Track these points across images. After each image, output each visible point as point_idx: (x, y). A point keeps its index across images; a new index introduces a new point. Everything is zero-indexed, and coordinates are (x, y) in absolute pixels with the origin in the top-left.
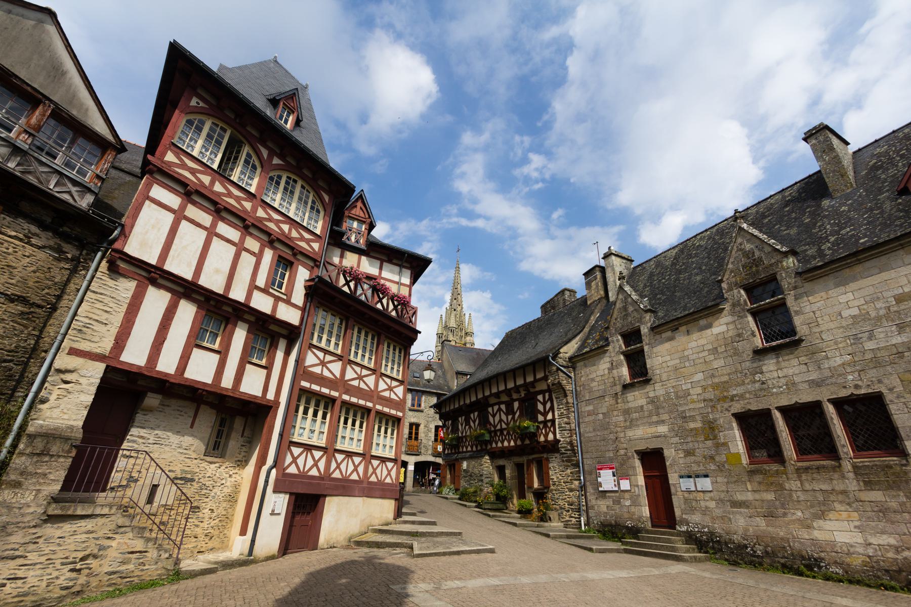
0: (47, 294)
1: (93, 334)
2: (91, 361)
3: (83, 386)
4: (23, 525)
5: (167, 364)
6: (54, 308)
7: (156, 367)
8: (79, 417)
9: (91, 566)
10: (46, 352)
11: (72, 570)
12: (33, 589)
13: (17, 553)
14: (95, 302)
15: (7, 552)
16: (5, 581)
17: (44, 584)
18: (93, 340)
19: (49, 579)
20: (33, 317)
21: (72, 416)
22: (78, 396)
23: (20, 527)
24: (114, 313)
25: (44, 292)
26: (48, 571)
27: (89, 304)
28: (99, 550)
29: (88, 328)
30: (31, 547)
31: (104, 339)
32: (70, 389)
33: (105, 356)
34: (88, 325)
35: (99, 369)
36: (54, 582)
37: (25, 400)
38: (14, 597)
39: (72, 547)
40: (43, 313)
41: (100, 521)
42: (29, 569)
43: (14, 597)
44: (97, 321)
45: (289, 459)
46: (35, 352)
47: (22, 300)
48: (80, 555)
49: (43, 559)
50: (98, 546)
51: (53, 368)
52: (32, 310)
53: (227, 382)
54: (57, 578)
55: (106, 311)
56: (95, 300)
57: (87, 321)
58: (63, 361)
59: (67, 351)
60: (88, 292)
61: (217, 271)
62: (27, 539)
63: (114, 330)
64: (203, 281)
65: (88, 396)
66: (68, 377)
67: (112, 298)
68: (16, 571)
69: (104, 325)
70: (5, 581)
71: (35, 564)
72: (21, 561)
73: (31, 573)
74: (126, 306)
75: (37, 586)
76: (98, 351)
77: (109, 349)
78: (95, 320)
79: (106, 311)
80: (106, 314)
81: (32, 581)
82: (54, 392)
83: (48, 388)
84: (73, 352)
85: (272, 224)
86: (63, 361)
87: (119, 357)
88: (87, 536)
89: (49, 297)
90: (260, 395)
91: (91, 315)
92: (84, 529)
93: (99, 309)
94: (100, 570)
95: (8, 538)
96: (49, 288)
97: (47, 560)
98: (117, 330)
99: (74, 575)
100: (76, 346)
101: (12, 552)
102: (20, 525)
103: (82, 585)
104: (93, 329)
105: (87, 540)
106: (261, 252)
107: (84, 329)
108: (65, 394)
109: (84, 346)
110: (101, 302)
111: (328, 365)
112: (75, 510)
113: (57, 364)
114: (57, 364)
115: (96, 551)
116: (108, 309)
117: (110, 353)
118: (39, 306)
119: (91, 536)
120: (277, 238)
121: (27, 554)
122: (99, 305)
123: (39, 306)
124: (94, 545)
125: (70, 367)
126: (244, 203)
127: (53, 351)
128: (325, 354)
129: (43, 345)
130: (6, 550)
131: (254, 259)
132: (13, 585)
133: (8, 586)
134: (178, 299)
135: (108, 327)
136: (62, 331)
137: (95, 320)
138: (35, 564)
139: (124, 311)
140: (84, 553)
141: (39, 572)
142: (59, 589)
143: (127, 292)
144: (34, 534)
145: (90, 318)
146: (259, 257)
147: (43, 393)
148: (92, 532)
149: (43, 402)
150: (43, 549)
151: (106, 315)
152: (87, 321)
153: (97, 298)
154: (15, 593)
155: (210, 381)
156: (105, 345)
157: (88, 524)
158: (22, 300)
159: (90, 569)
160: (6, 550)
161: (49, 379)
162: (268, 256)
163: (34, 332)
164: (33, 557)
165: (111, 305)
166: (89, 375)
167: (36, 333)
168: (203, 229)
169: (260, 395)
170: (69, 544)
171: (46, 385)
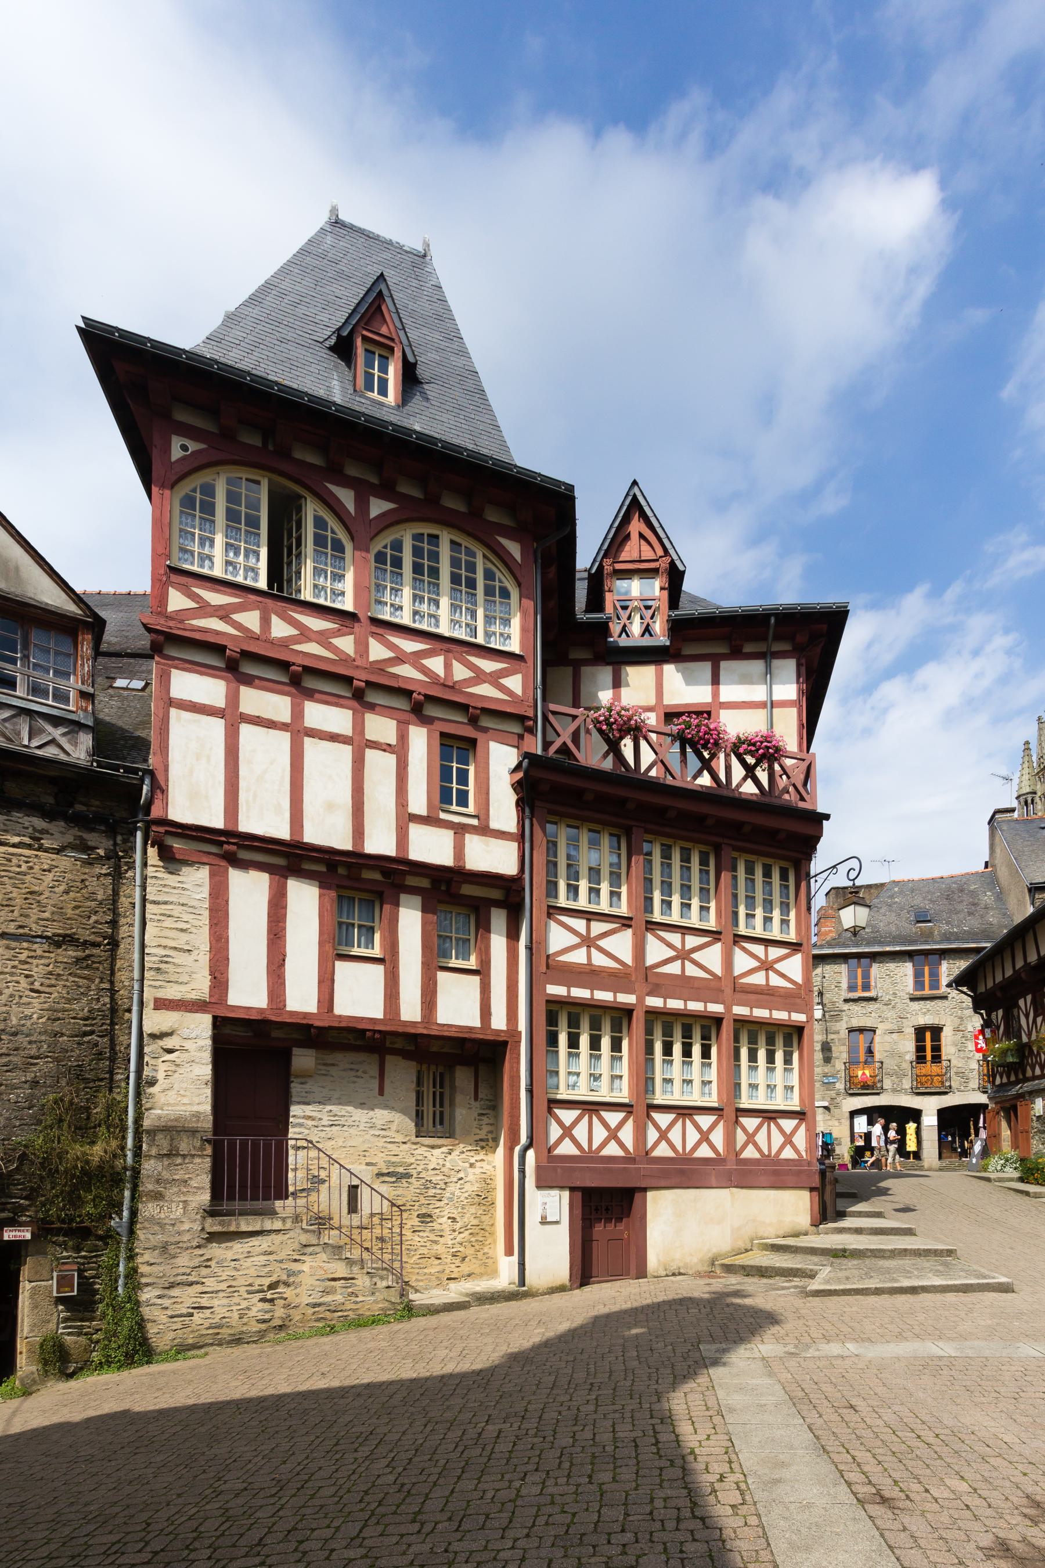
2: (188, 1014)
8: (202, 1098)
10: (129, 1011)
12: (224, 1320)
13: (191, 1279)
15: (180, 1277)
24: (193, 930)
27: (155, 924)
29: (166, 962)
31: (194, 976)
33: (205, 1001)
35: (201, 1026)
37: (128, 1084)
38: (207, 1329)
43: (207, 1329)
44: (175, 948)
45: (555, 1132)
46: (115, 1013)
54: (248, 1309)
55: (182, 930)
56: (161, 915)
57: (162, 952)
59: (152, 1006)
63: (204, 959)
64: (312, 836)
66: (168, 1043)
68: (199, 1300)
69: (187, 954)
71: (217, 1292)
72: (199, 1288)
73: (216, 1302)
74: (206, 913)
76: (193, 996)
77: (207, 990)
78: (171, 948)
79: (182, 930)
80: (183, 934)
81: (221, 1312)
82: (158, 1067)
83: (150, 1063)
84: (161, 1004)
86: (154, 1021)
91: (164, 942)
92: (258, 1250)
95: (173, 1261)
100: (161, 994)
101: (185, 1277)
104: (174, 964)
106: (403, 737)
107: (163, 966)
109: (172, 992)
110: (169, 916)
111: (601, 943)
112: (238, 1225)
113: (147, 1029)
116: (184, 926)
117: (210, 996)
120: (426, 696)
121: (204, 1280)
122: (169, 923)
125: (165, 1028)
126: (338, 642)
127: (135, 1008)
128: (589, 920)
130: (178, 1275)
131: (391, 760)
134: (282, 879)
136: (136, 975)
137: (171, 948)
139: (207, 922)
143: (201, 889)
145: (165, 947)
146: (400, 750)
147: (147, 1072)
149: (152, 1083)
151: (185, 937)
152: (162, 952)
154: (207, 1325)
160: (178, 1275)
161: (146, 1050)
162: (419, 739)
163: (103, 986)
164: (211, 1284)
166: (193, 1035)
167: (106, 986)
168: (280, 729)
171: (146, 1059)
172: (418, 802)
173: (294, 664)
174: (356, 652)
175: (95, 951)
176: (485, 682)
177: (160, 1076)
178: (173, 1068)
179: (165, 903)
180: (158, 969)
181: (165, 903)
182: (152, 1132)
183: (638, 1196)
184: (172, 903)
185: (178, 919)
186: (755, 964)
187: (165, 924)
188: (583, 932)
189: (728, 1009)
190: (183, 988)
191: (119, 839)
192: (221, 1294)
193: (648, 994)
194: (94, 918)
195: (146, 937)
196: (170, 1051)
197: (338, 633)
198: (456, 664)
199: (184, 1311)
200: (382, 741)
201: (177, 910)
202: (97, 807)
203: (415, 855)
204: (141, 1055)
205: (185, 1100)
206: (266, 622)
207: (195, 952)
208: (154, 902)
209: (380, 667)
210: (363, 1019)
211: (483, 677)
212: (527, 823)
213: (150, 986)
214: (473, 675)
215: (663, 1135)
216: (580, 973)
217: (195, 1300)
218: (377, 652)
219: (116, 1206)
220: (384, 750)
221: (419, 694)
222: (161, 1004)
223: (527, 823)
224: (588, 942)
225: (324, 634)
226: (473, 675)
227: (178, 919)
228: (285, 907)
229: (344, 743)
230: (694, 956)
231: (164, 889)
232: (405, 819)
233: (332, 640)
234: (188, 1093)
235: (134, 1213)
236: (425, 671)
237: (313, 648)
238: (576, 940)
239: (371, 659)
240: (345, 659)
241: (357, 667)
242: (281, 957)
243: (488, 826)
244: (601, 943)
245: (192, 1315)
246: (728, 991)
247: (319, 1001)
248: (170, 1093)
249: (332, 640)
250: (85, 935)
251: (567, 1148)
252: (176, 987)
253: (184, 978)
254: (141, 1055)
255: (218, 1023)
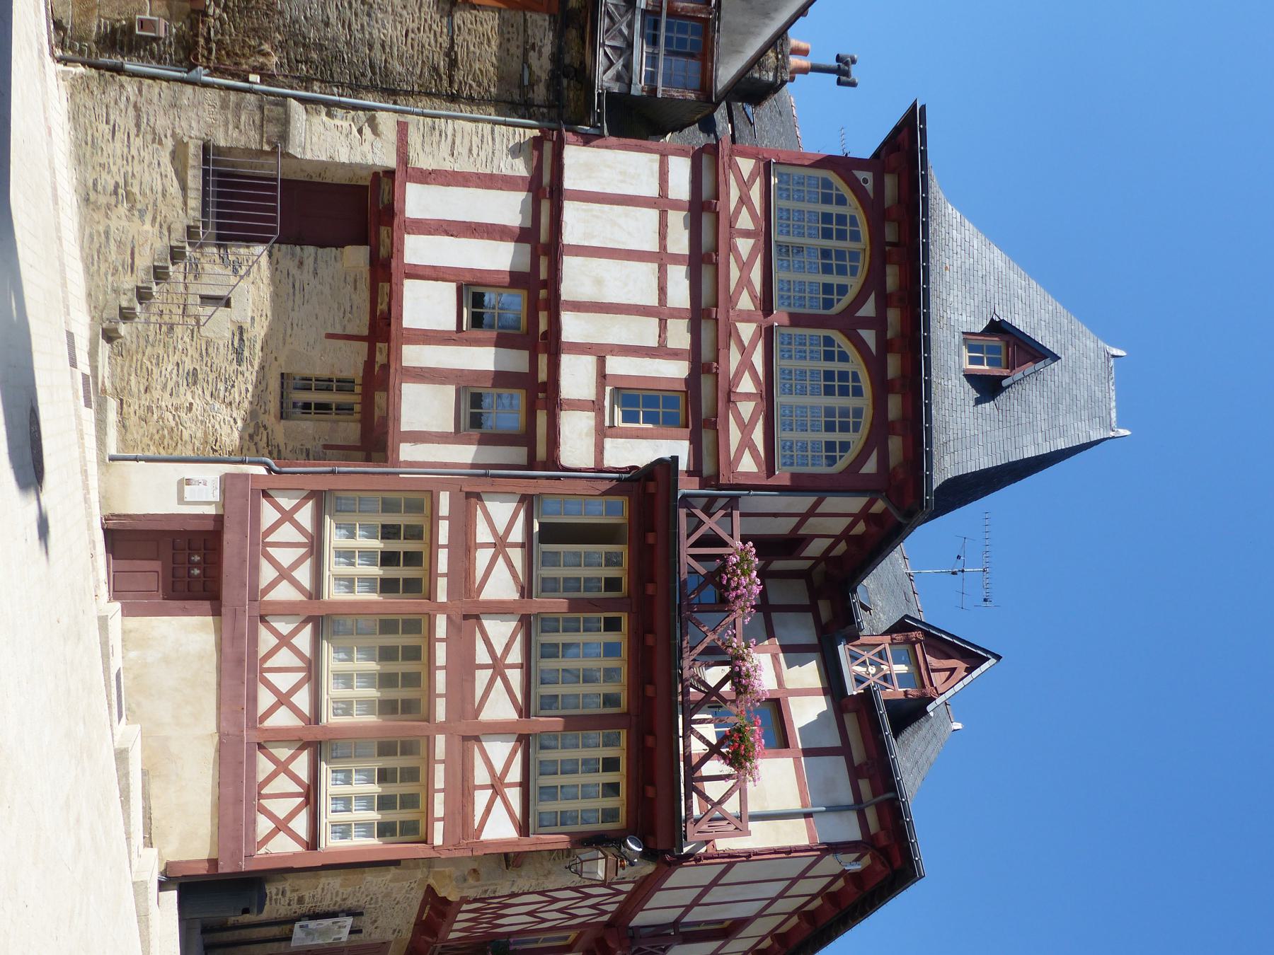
0: (470, 85)
1: (434, 142)
2: (395, 148)
3: (359, 149)
4: (177, 123)
5: (417, 250)
6: (453, 98)
7: (409, 233)
8: (317, 152)
9: (119, 206)
10: (395, 103)
11: (117, 185)
13: (143, 126)
14: (480, 135)
15: (145, 116)
16: (112, 123)
17: (103, 160)
18: (425, 145)
19: (109, 164)
20: (436, 81)
21: (317, 146)
22: (345, 146)
23: (175, 120)
25: (471, 82)
26: (119, 162)
27: (474, 130)
28: (140, 211)
29: (440, 135)
30: (149, 137)
31: (430, 157)
32: (352, 135)
33: (406, 164)
34: (443, 135)
36: (104, 169)
37: (328, 94)
39: (146, 178)
40: (444, 89)
41: (178, 203)
42: (123, 143)
46: (391, 93)
47: (453, 64)
48: (136, 190)
49: (134, 152)
50: (144, 208)
51: (373, 112)
52: (444, 77)
53: (413, 355)
55: (470, 150)
56: (483, 136)
57: (450, 132)
58: (387, 121)
59: (401, 119)
60: (489, 126)
61: (599, 282)
62: (159, 130)
63: (448, 165)
64: (570, 265)
65: (347, 156)
66: (367, 130)
67: (493, 152)
68: (122, 130)
70: (112, 123)
71: (129, 147)
72: (133, 131)
73: (118, 144)
74: (488, 171)
75: (102, 153)
76: (412, 154)
77: (418, 165)
79: (470, 150)
80: (467, 151)
81: (108, 149)
82: (343, 121)
83: (349, 115)
84: (402, 129)
85: (739, 357)
86: (387, 121)
87: (410, 181)
88: (160, 190)
89: (467, 88)
90: (404, 428)
91: (459, 136)
93: (471, 141)
94: (114, 217)
95: (162, 112)
96: (479, 85)
97: (133, 157)
98: (448, 169)
99: (111, 188)
101: (145, 121)
102: (177, 119)
103: (96, 202)
104: (440, 141)
105: (154, 192)
106: (675, 354)
108: (344, 131)
109: (414, 138)
113: (380, 115)
114: (380, 115)
115: (139, 206)
117: (413, 168)
118: (451, 83)
119: (159, 196)
121: (141, 136)
122: (476, 140)
123: (451, 83)
124: (147, 202)
125: (381, 128)
129: (400, 99)
131: (653, 342)
132: (107, 130)
133: (107, 127)
135: (449, 158)
136: (427, 111)
138: (129, 147)
139: (480, 171)
140: (138, 193)
141: (119, 153)
142: (95, 177)
143: (509, 168)
144: (166, 136)
145: (454, 135)
146: (661, 351)
147: (340, 112)
148: (164, 195)
149: (329, 114)
150: (146, 149)
151: (465, 152)
152: (450, 132)
153: (485, 136)
155: (406, 324)
156: (422, 159)
157: (174, 188)
158: (453, 64)
159: (116, 206)
160: (148, 115)
161: (361, 113)
165: (482, 154)
167: (416, 88)
169: (404, 428)
170: (150, 174)
171: (353, 113)
172: (616, 366)
173: (717, 255)
174: (740, 310)
175: (445, 83)
176: (742, 434)
177: (338, 122)
178: (344, 132)
179: (493, 139)
180: (434, 129)
181: (493, 139)
182: (284, 106)
183: (207, 605)
184: (494, 144)
185: (480, 148)
186: (499, 767)
187: (474, 138)
188: (511, 539)
189: (441, 728)
190: (419, 147)
191: (545, 110)
192: (126, 150)
193: (449, 618)
194: (474, 85)
195: (461, 121)
196: (360, 131)
197: (753, 297)
198: (752, 405)
199: (112, 118)
200: (668, 334)
201: (488, 147)
202: (568, 96)
203: (566, 360)
204: (355, 108)
205: (315, 139)
206: (746, 234)
207: (452, 160)
208: (493, 131)
209: (731, 332)
210: (401, 306)
211: (746, 432)
212: (617, 475)
213: (419, 120)
214: (746, 421)
215: (284, 641)
216: (466, 534)
217: (122, 127)
218: (747, 331)
219: (215, 71)
220: (660, 336)
221: (717, 368)
222: (402, 129)
223: (617, 475)
224: (500, 545)
225: (749, 284)
226: (746, 421)
227: (480, 148)
228: (502, 240)
229: (660, 300)
230: (499, 682)
231: (505, 140)
232: (600, 352)
233: (745, 289)
234: (321, 141)
235: (206, 85)
236: (739, 375)
237: (735, 273)
238: (501, 531)
239: (738, 324)
240: (732, 300)
241: (728, 311)
242: (455, 233)
243: (605, 436)
244: (501, 560)
245: (107, 123)
246: (465, 728)
247: (415, 265)
248: (322, 128)
249: (745, 289)
250: (459, 75)
251: (269, 515)
252: (419, 141)
253: (427, 148)
254: (355, 108)
255: (390, 173)
